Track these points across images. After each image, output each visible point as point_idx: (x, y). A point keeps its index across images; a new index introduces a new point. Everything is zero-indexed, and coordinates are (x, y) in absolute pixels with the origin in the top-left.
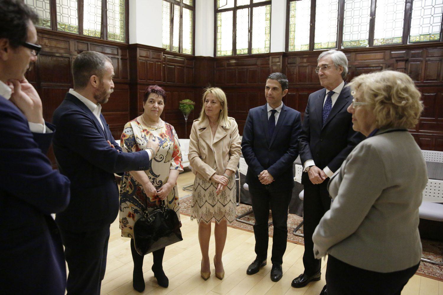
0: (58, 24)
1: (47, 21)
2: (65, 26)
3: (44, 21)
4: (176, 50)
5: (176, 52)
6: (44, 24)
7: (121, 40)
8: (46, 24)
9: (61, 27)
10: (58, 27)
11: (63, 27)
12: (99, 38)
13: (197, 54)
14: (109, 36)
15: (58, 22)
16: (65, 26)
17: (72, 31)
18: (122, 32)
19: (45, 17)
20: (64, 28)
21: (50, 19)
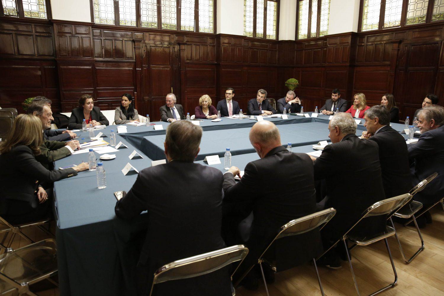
1: (424, 17)
3: (421, 18)
8: (422, 20)
9: (436, 18)
16: (441, 15)
20: (438, 18)
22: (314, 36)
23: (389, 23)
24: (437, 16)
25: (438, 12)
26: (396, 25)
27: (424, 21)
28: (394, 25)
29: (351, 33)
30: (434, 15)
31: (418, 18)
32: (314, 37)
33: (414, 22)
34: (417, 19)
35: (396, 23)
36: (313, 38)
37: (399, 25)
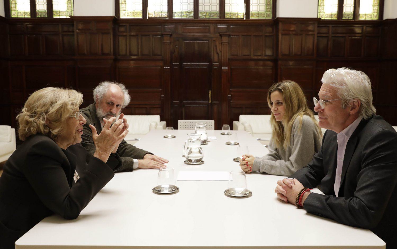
0: (199, 13)
1: (191, 12)
2: (206, 13)
3: (188, 12)
4: (349, 18)
5: (348, 20)
6: (187, 15)
7: (267, 17)
9: (203, 15)
10: (200, 15)
11: (205, 14)
12: (242, 19)
13: (385, 17)
14: (252, 15)
15: (200, 11)
16: (206, 13)
17: (212, 17)
18: (268, 8)
19: (189, 10)
20: (205, 15)
21: (193, 11)
22: (42, 16)
23: (155, 13)
24: (203, 13)
25: (203, 10)
26: (163, 16)
27: (192, 16)
28: (161, 16)
29: (113, 18)
30: (201, 13)
31: (186, 13)
32: (43, 18)
33: (183, 16)
34: (185, 13)
35: (162, 13)
36: (41, 18)
37: (167, 16)
